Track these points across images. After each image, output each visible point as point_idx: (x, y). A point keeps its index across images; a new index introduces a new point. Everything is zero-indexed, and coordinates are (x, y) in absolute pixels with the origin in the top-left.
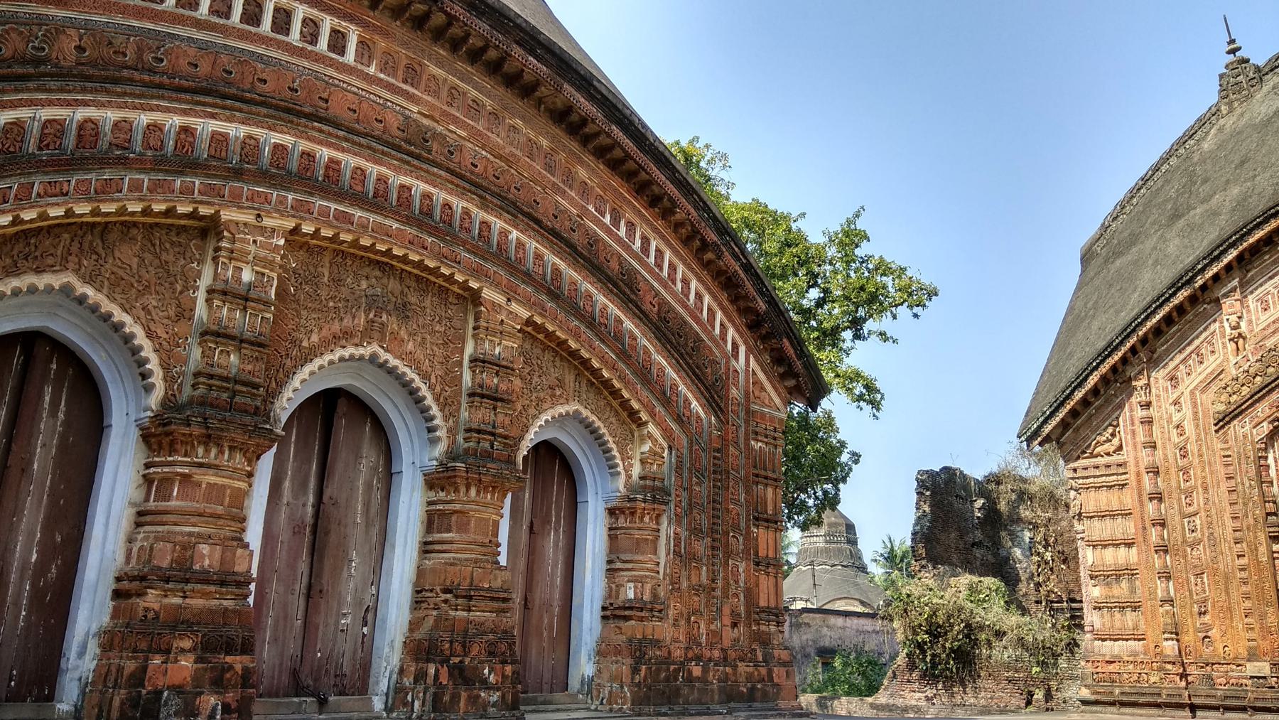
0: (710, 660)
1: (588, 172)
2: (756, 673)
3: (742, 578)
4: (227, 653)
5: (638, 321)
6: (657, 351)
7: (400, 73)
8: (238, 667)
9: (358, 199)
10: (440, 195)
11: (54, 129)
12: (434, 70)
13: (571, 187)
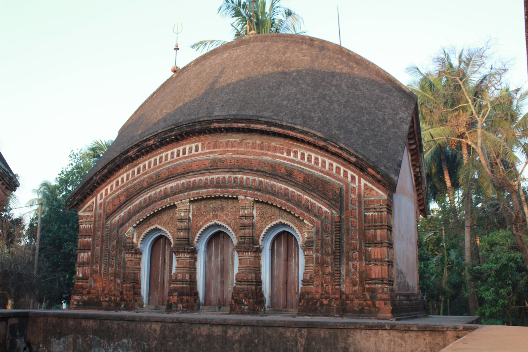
0: (333, 298)
1: (275, 143)
2: (365, 303)
3: (358, 267)
4: (183, 296)
5: (294, 187)
6: (304, 194)
7: (212, 147)
8: (185, 299)
9: (201, 187)
10: (221, 176)
11: (145, 200)
12: (221, 140)
13: (270, 151)
